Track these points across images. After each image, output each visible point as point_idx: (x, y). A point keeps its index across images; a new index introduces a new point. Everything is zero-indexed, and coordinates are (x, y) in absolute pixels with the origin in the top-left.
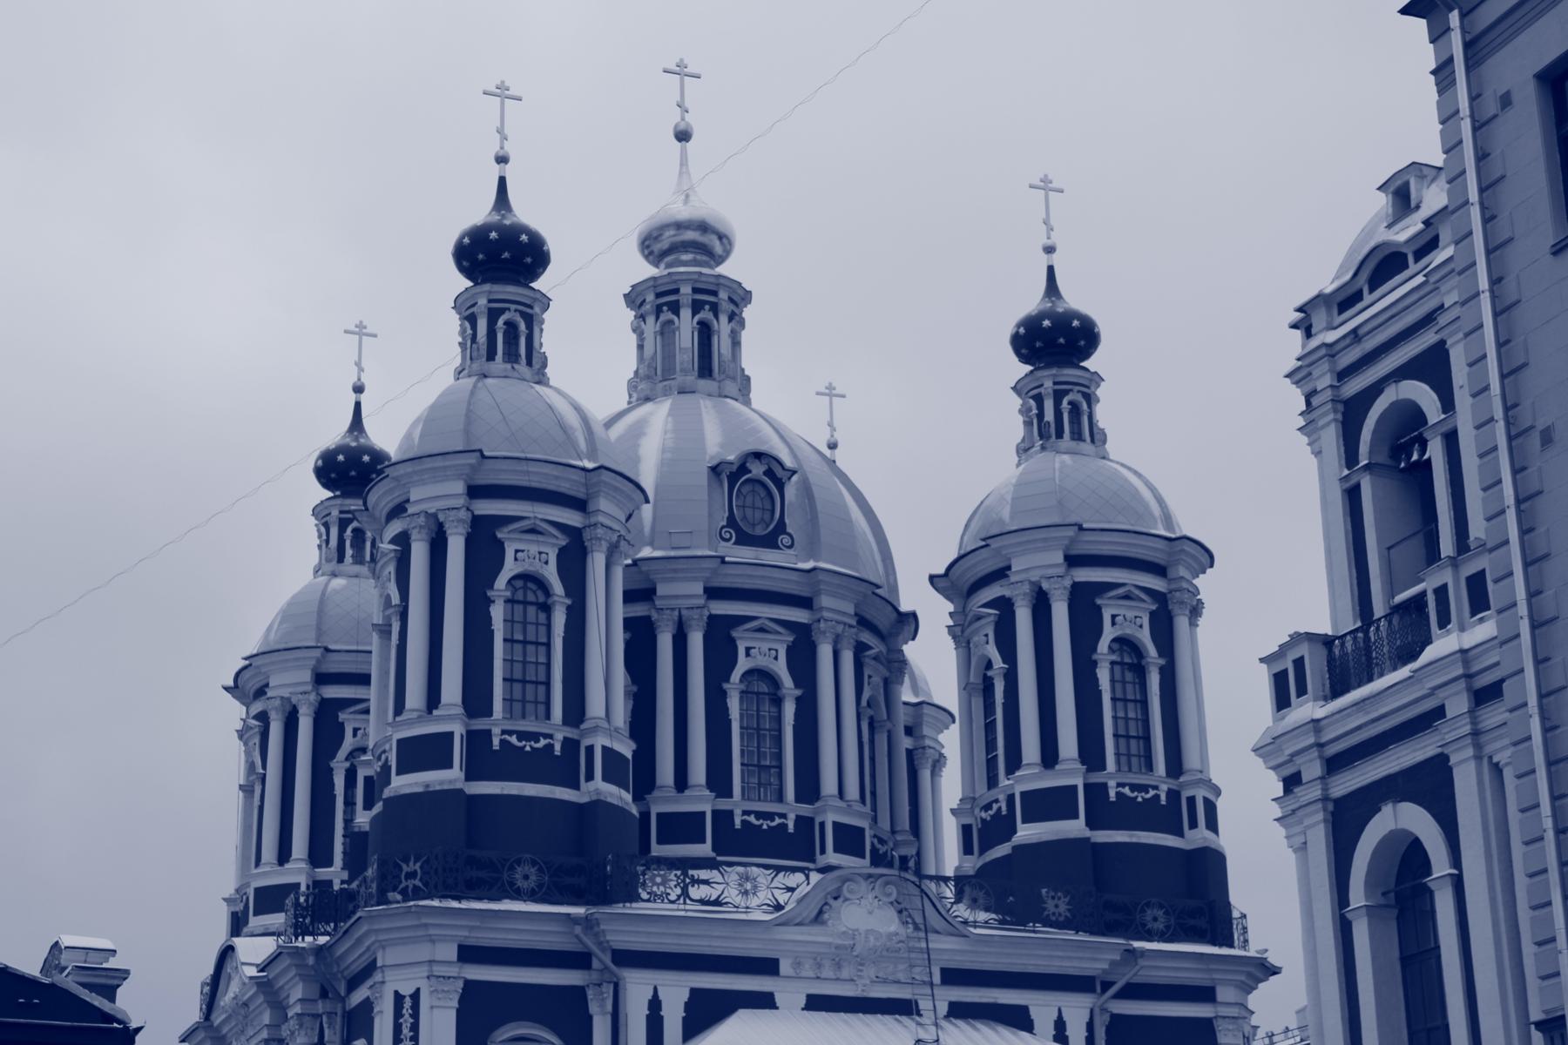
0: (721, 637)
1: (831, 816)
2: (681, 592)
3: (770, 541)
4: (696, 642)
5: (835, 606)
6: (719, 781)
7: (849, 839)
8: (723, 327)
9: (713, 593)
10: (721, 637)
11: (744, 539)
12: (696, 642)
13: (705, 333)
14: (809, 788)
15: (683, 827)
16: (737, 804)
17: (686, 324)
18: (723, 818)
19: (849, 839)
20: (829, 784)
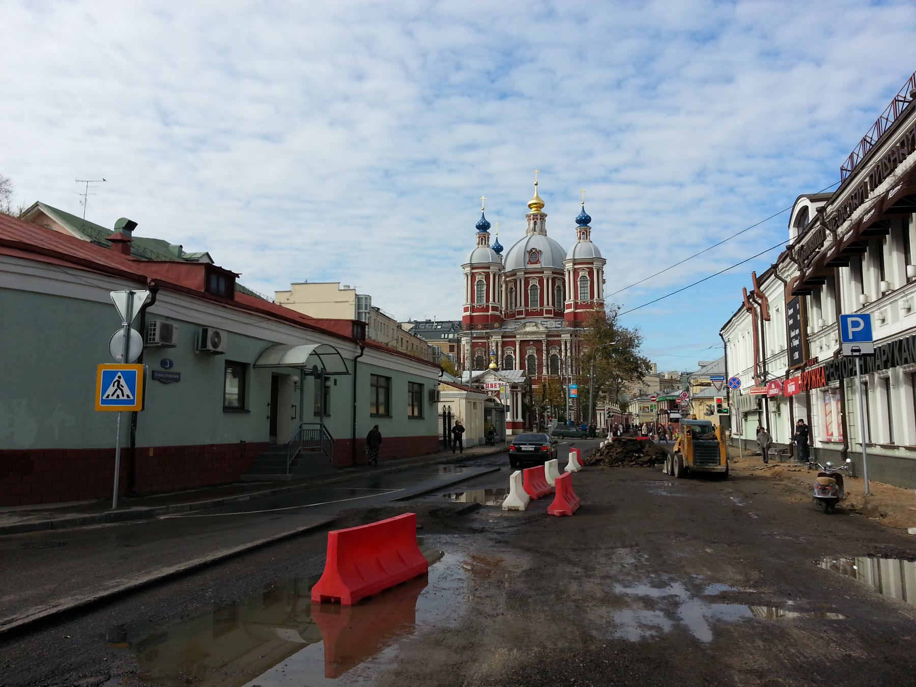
0: (527, 281)
1: (545, 308)
2: (521, 274)
3: (536, 263)
4: (523, 282)
5: (547, 273)
6: (526, 305)
7: (548, 312)
8: (539, 222)
9: (525, 273)
10: (527, 281)
11: (532, 263)
12: (523, 282)
13: (535, 223)
14: (542, 304)
15: (520, 313)
16: (529, 308)
17: (532, 222)
18: (527, 311)
19: (548, 312)
20: (545, 303)
